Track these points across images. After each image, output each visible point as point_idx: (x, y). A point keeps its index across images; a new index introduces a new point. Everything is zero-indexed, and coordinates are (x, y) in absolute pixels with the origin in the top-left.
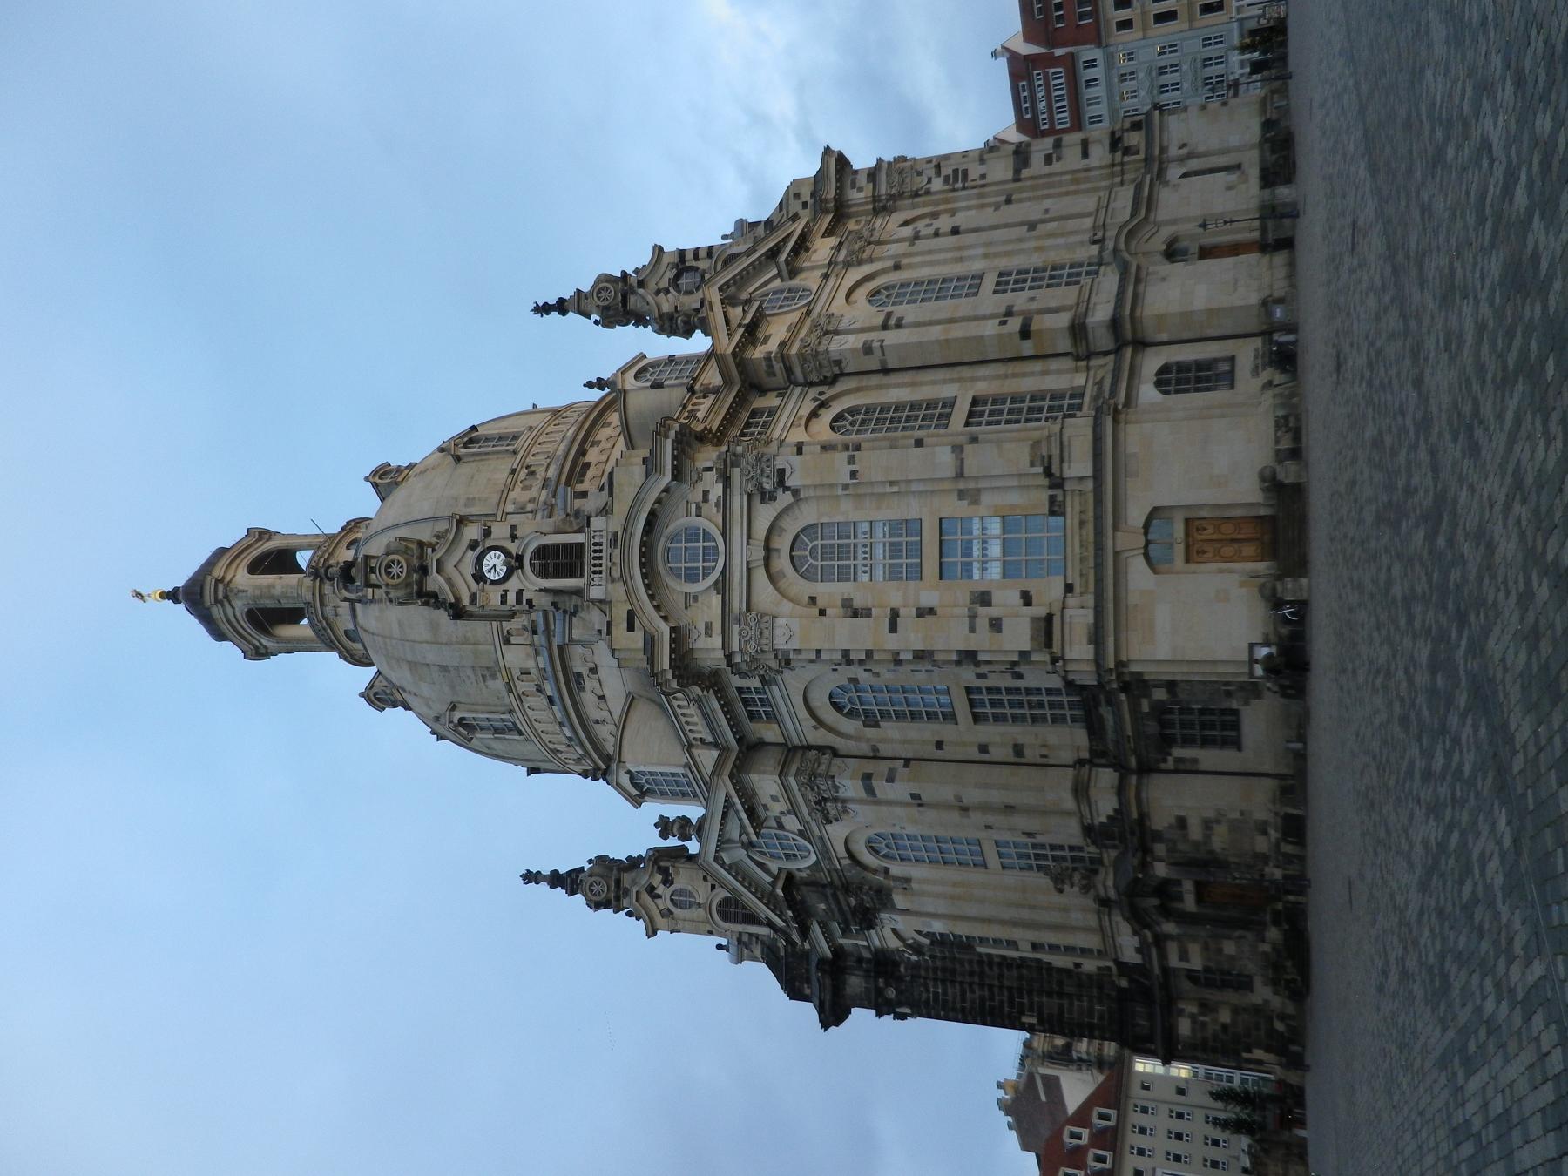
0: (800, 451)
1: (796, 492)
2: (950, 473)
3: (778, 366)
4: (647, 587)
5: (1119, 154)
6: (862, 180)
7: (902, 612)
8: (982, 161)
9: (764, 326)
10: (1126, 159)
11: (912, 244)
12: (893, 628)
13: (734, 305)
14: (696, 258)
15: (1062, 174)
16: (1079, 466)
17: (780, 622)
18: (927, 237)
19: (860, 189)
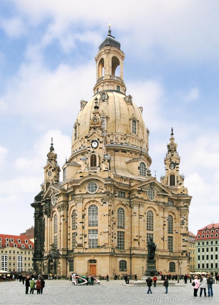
0: (109, 206)
1: (102, 205)
2: (104, 231)
3: (133, 196)
4: (86, 180)
5: (182, 252)
6: (185, 204)
7: (83, 224)
8: (185, 227)
9: (143, 192)
10: (181, 253)
11: (162, 217)
12: (80, 223)
13: (150, 185)
14: (177, 168)
15: (180, 242)
16: (103, 250)
17: (81, 204)
18: (164, 220)
19: (183, 204)
